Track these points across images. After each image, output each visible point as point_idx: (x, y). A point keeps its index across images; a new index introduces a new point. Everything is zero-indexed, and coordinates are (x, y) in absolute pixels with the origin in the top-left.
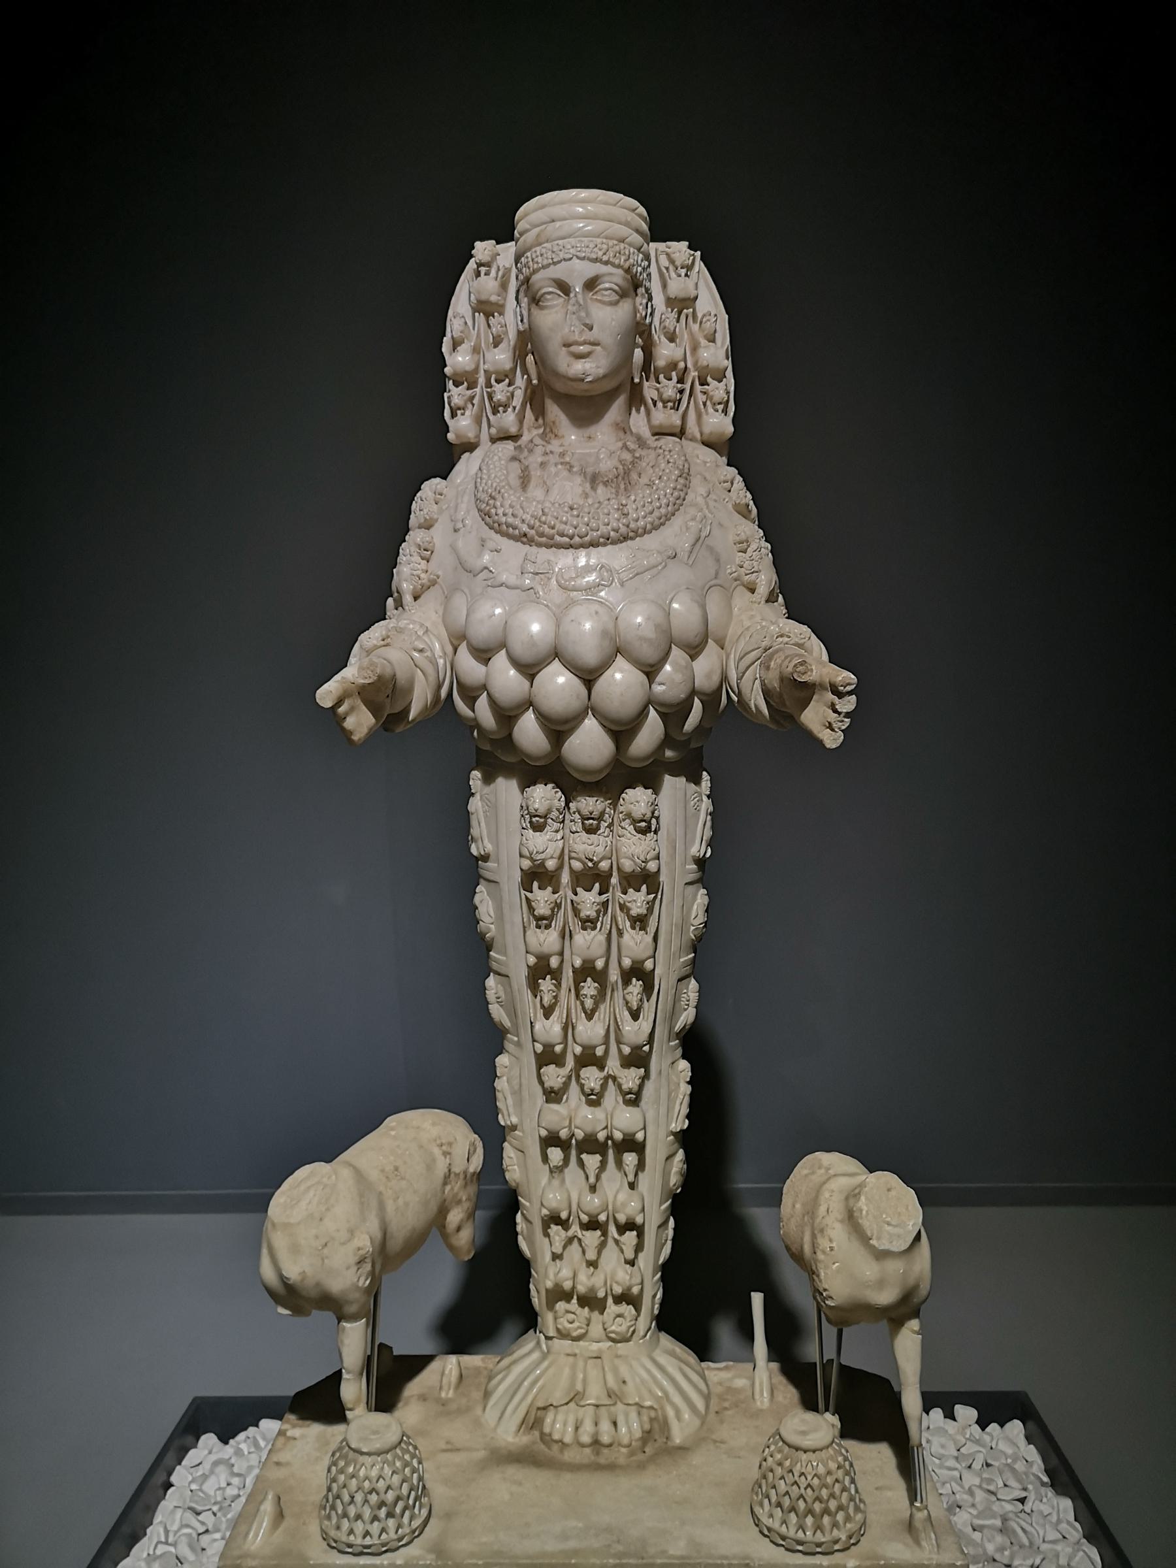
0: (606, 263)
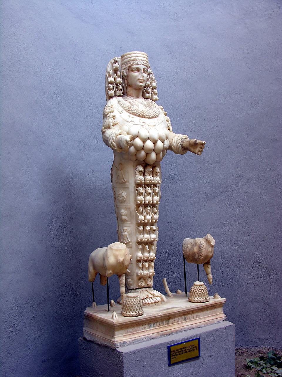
0: (146, 66)
